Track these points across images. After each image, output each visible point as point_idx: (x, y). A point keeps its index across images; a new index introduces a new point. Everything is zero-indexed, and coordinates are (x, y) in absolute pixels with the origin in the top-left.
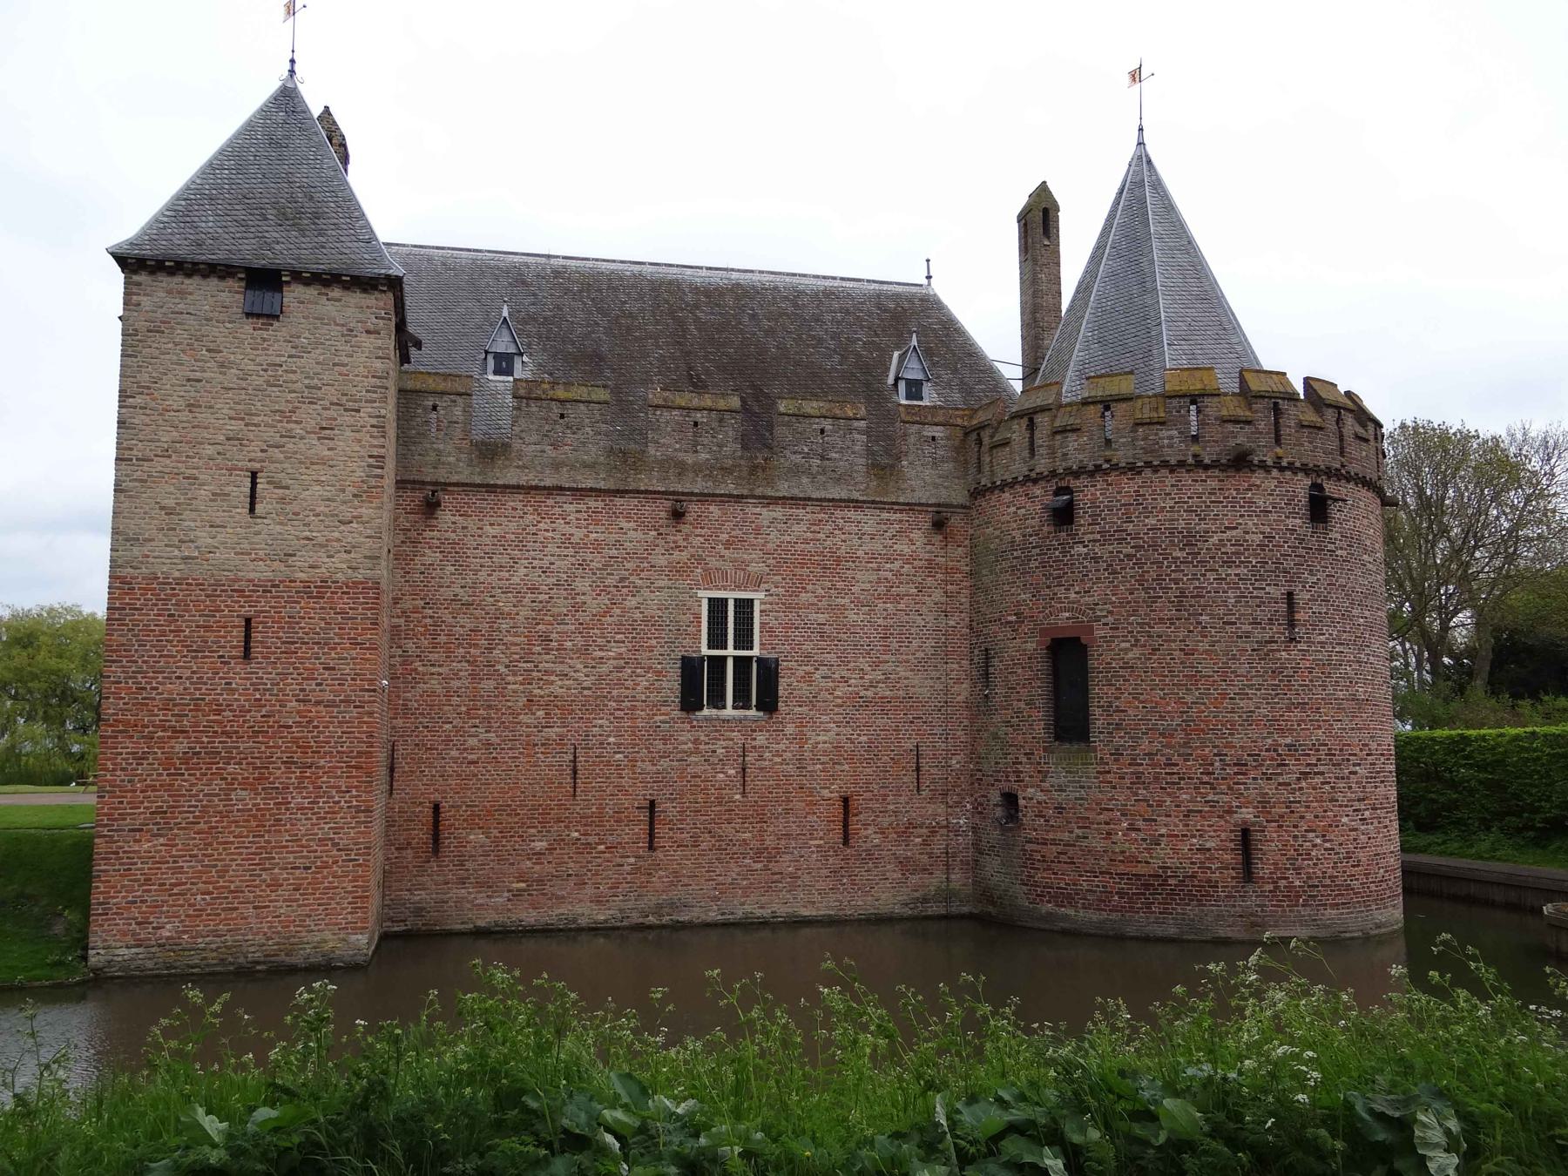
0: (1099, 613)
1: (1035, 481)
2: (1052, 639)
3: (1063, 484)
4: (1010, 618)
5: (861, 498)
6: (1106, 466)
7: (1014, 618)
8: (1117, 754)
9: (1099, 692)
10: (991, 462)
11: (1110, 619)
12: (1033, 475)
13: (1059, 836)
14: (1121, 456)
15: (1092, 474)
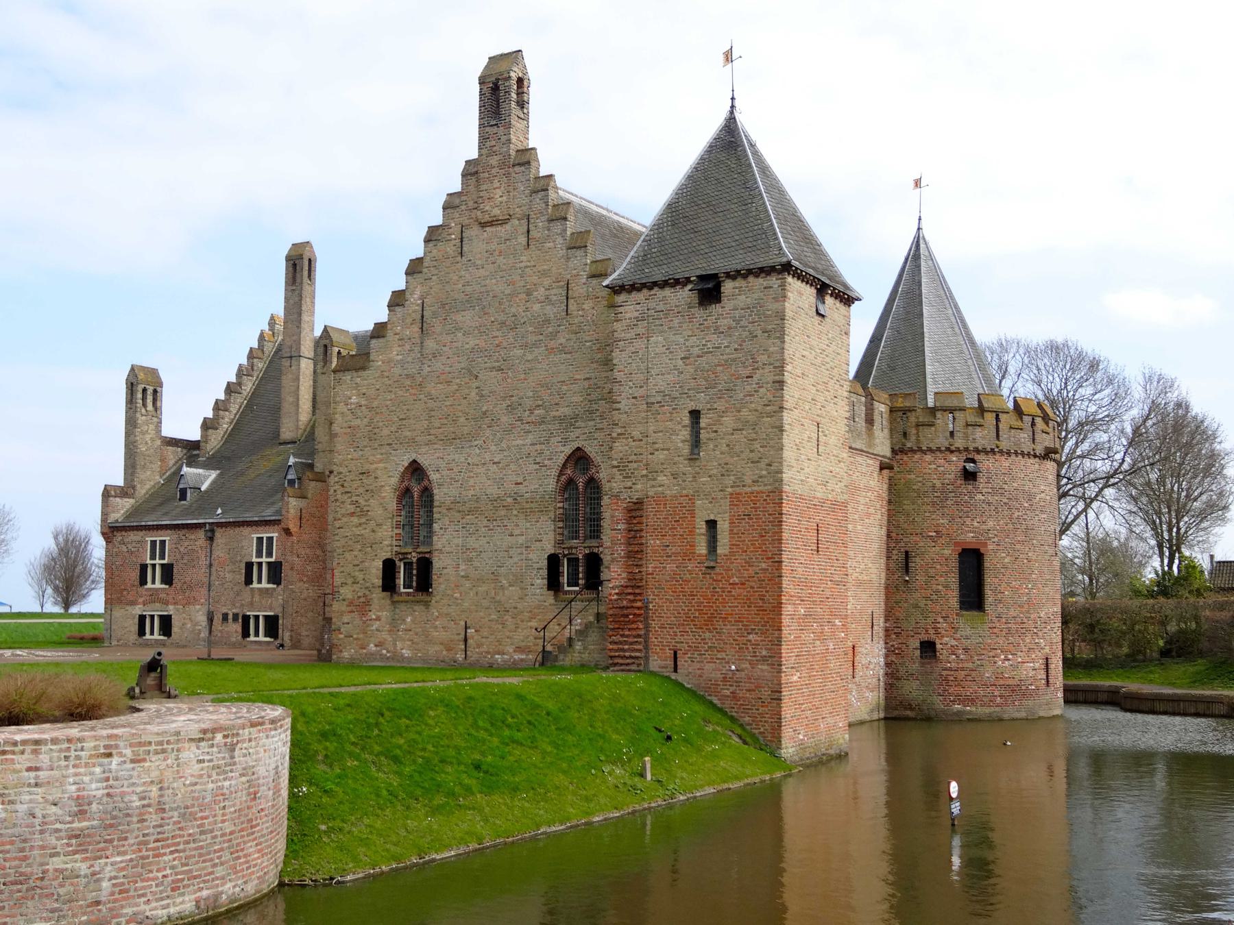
0: (990, 536)
1: (952, 452)
2: (963, 549)
3: (970, 456)
4: (931, 534)
5: (865, 449)
6: (996, 450)
7: (934, 534)
8: (999, 617)
9: (990, 580)
10: (917, 433)
11: (996, 540)
12: (953, 448)
13: (966, 665)
14: (1004, 444)
15: (987, 453)
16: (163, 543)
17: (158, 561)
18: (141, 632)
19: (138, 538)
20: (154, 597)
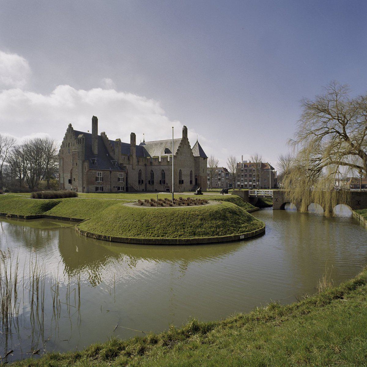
16: (101, 173)
17: (99, 177)
18: (96, 190)
19: (95, 172)
20: (99, 183)
